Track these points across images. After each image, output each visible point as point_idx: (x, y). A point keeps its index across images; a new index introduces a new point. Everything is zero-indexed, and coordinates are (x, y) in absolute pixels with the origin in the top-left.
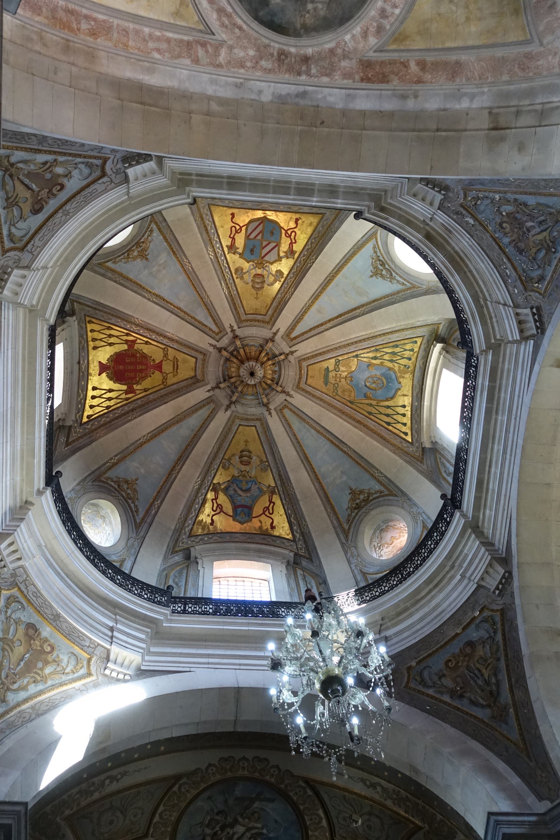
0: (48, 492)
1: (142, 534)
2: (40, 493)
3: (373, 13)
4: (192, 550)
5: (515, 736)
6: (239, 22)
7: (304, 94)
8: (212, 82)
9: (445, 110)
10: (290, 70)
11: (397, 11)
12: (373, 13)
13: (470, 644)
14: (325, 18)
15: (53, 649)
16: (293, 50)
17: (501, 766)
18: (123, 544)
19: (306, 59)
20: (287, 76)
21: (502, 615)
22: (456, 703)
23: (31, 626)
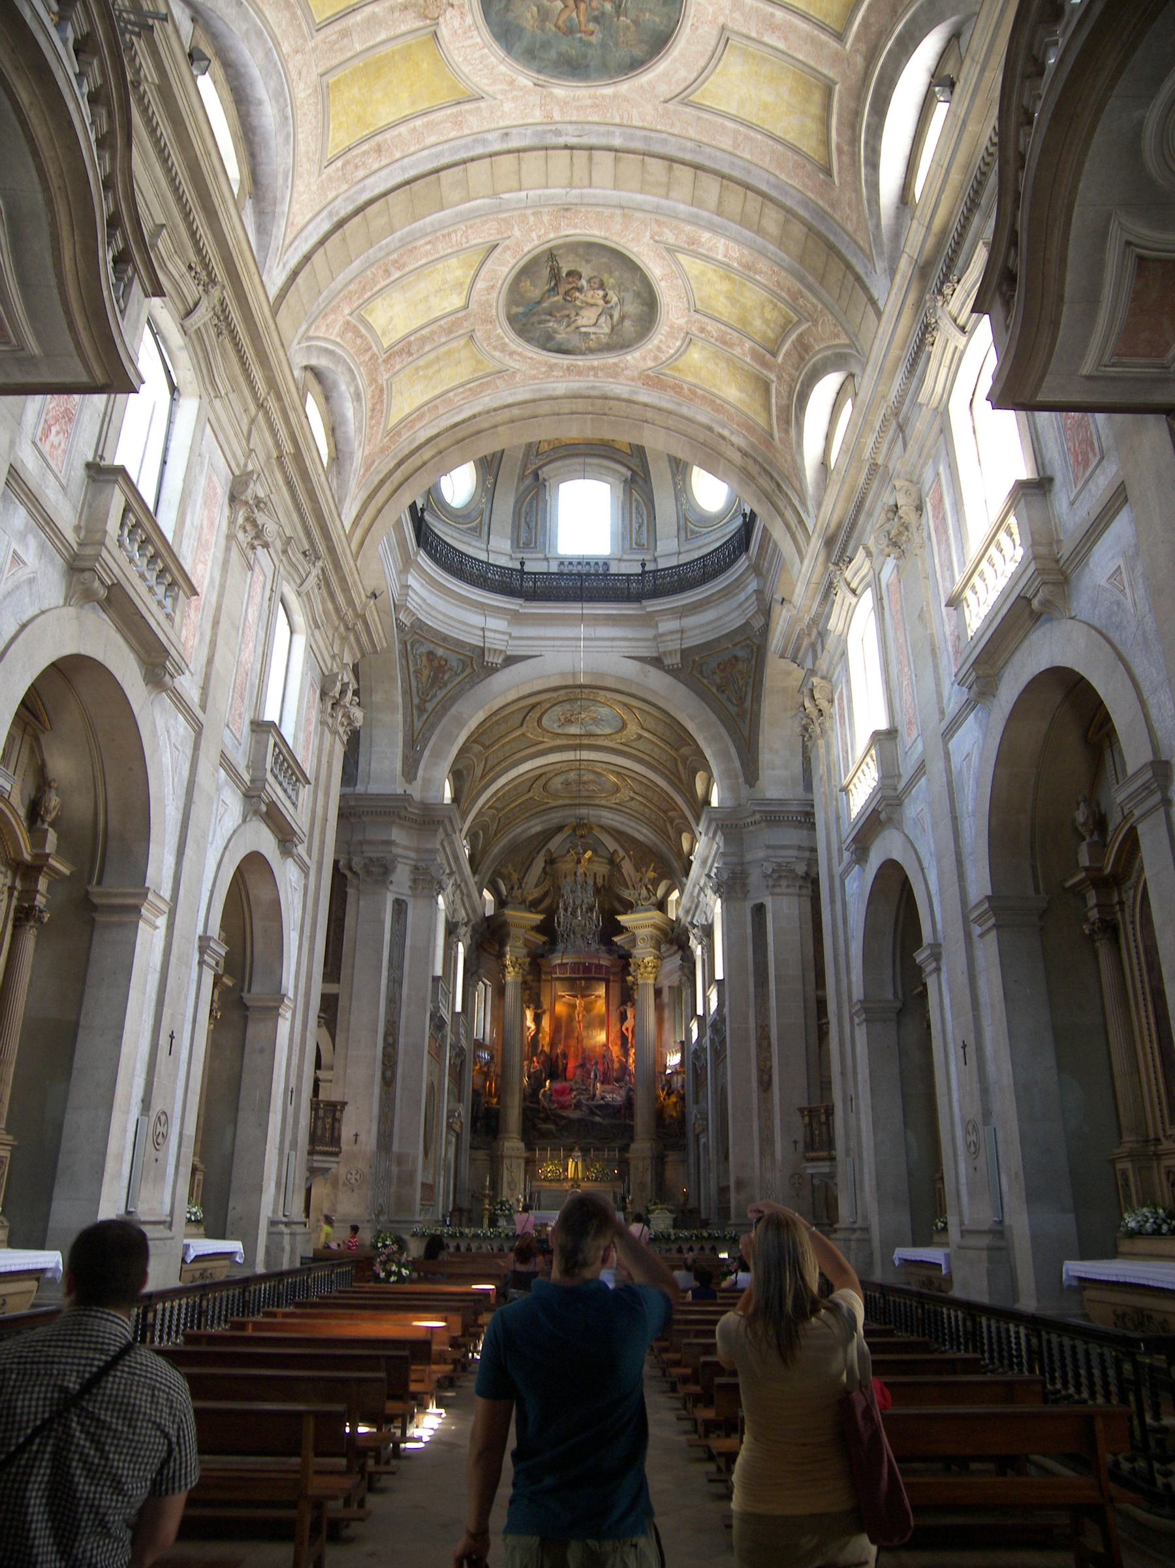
0: (422, 552)
1: (495, 471)
2: (417, 554)
3: (650, 347)
4: (540, 472)
5: (746, 733)
6: (530, 354)
7: (593, 388)
8: (511, 394)
9: (710, 429)
10: (580, 373)
11: (672, 351)
12: (650, 347)
13: (736, 658)
14: (607, 344)
15: (446, 661)
16: (581, 363)
17: (733, 751)
18: (480, 491)
19: (593, 368)
20: (577, 378)
21: (758, 648)
22: (719, 695)
23: (430, 654)
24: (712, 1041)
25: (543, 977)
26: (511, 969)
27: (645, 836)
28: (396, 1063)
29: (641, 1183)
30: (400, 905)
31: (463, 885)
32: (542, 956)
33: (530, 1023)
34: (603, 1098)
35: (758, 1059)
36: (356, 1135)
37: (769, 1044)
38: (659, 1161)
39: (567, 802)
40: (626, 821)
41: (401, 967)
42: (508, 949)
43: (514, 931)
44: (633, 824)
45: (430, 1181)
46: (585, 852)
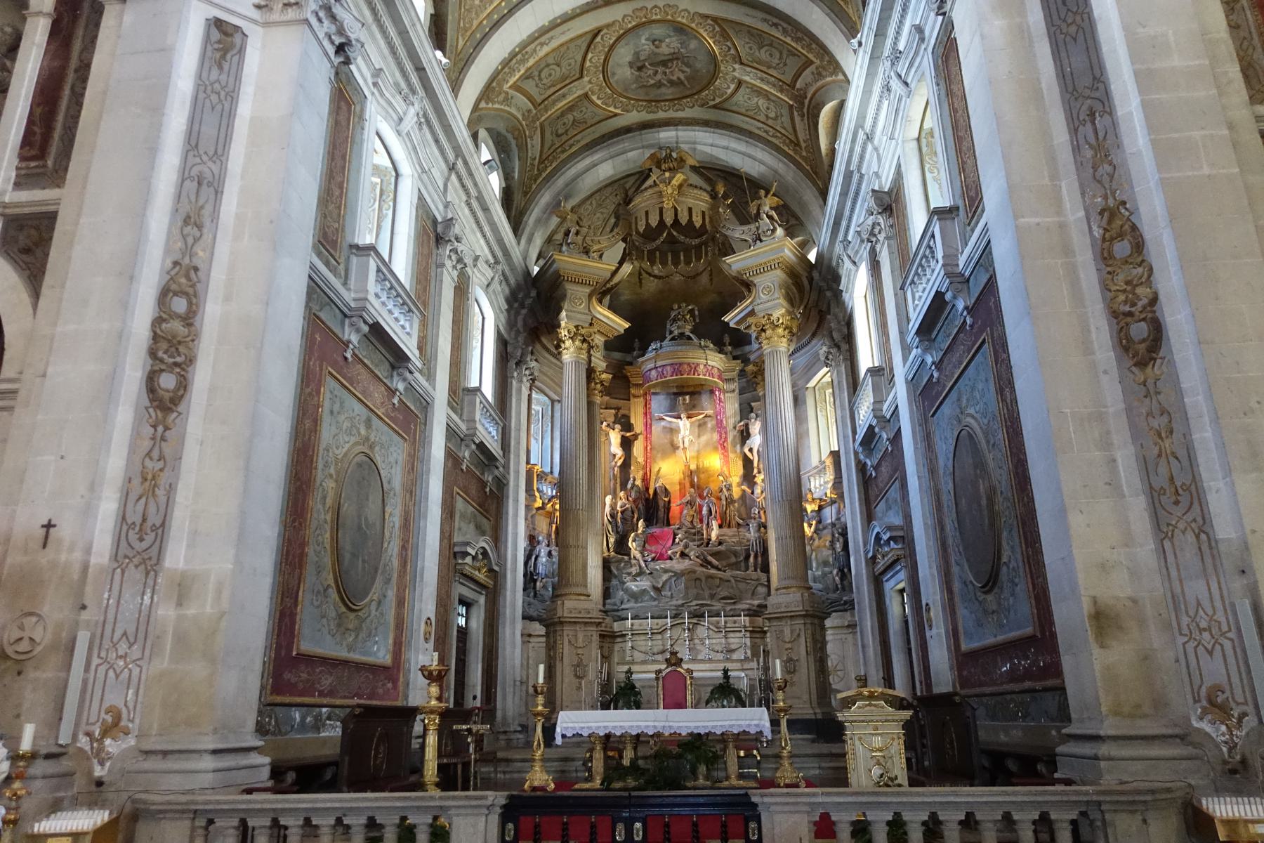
24: (911, 382)
25: (633, 391)
26: (568, 343)
27: (761, 162)
28: (191, 361)
29: (790, 660)
30: (226, 34)
31: (460, 164)
32: (631, 364)
33: (616, 448)
34: (720, 543)
35: (1105, 288)
36: (49, 526)
37: (1139, 245)
38: (816, 616)
39: (645, 116)
40: (734, 144)
41: (220, 154)
42: (564, 314)
43: (571, 289)
44: (741, 147)
45: (381, 654)
46: (671, 179)
